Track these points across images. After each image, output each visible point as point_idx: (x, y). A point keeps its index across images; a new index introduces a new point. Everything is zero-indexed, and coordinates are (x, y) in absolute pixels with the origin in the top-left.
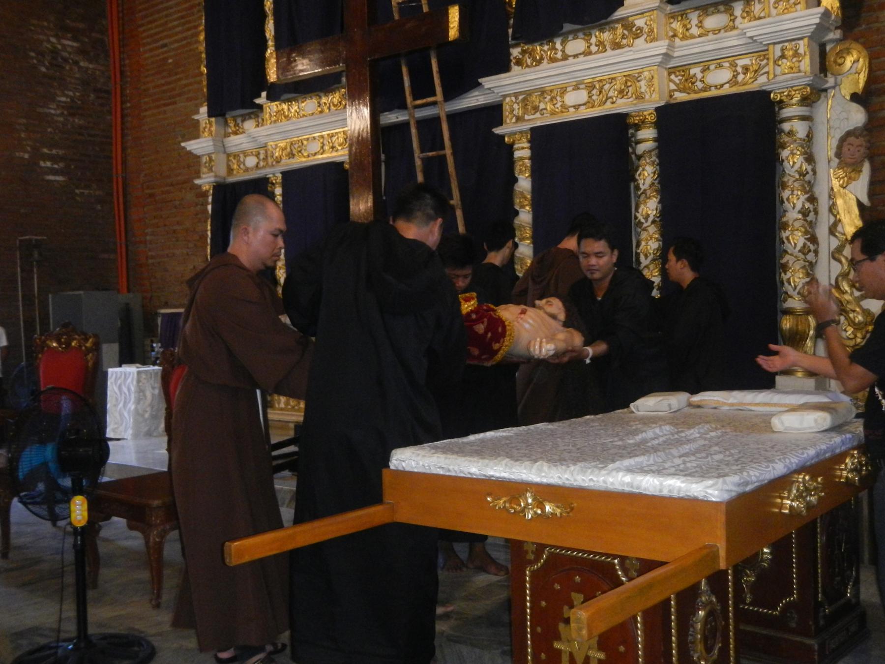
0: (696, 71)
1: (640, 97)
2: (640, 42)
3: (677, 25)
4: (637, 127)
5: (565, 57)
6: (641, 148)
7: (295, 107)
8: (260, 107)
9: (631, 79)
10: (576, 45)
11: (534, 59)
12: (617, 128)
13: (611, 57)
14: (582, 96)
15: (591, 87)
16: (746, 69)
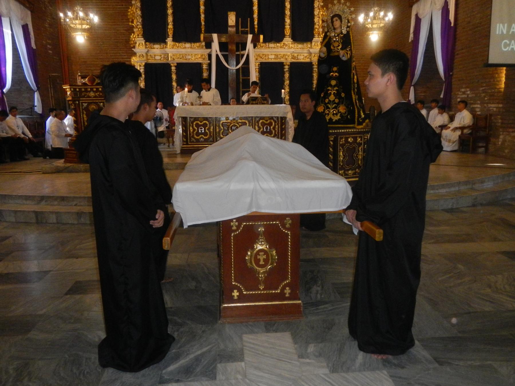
0: (296, 55)
1: (286, 59)
2: (287, 47)
3: (293, 46)
4: (285, 65)
5: (269, 48)
6: (285, 70)
7: (180, 44)
8: (166, 43)
9: (284, 55)
10: (272, 45)
11: (261, 46)
12: (282, 64)
13: (280, 50)
14: (273, 57)
15: (275, 55)
16: (306, 57)
